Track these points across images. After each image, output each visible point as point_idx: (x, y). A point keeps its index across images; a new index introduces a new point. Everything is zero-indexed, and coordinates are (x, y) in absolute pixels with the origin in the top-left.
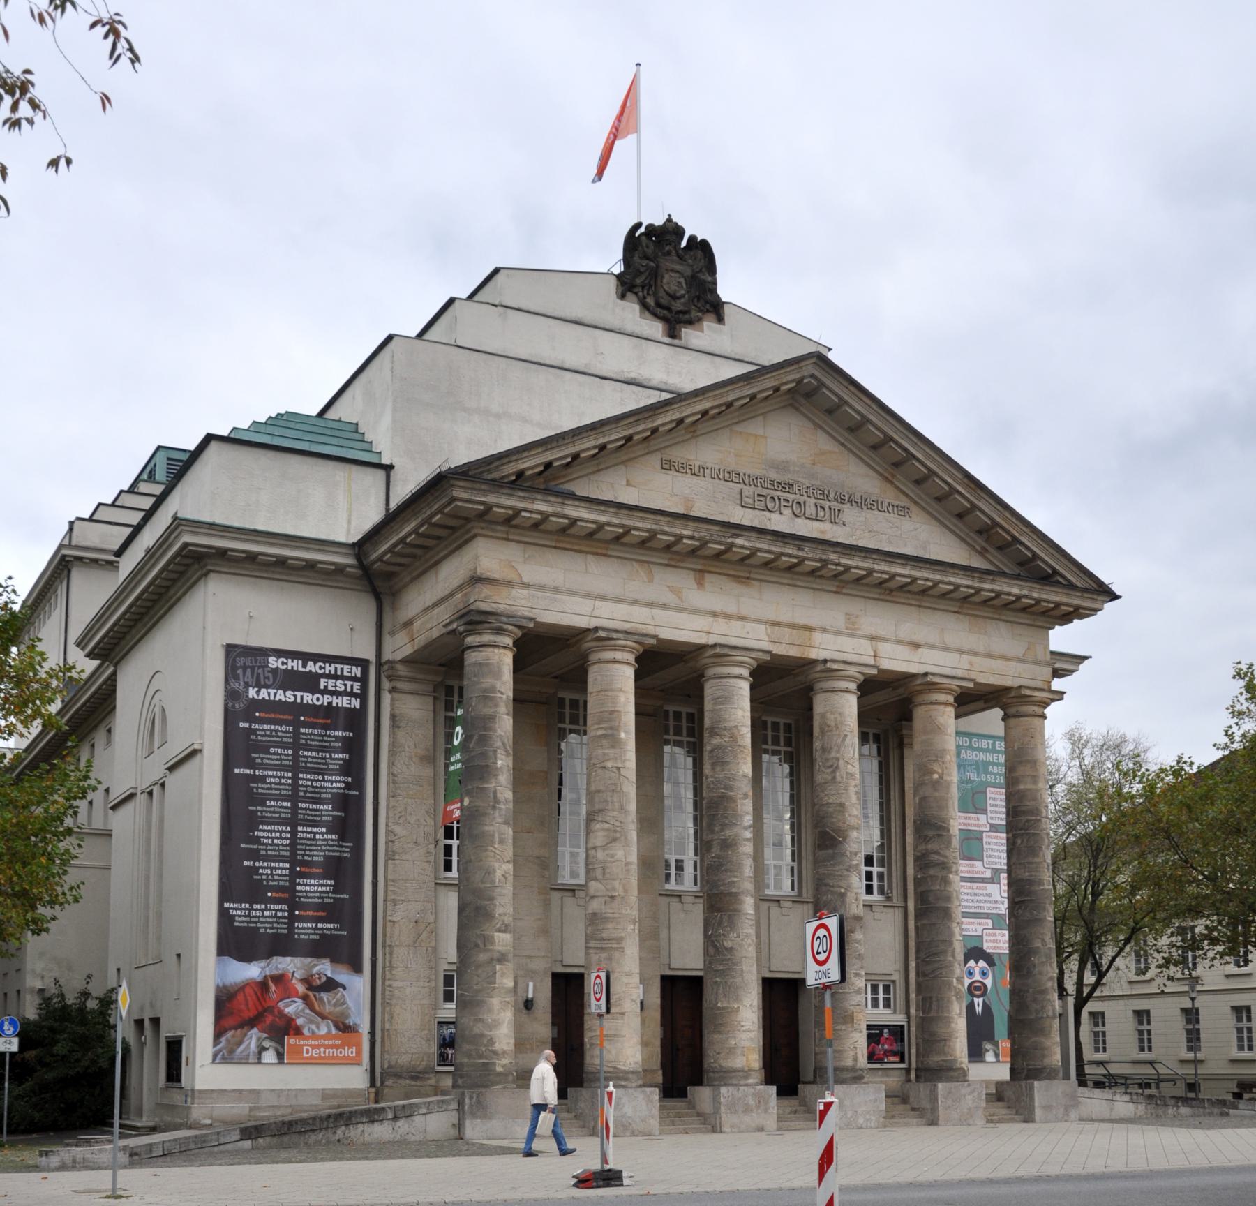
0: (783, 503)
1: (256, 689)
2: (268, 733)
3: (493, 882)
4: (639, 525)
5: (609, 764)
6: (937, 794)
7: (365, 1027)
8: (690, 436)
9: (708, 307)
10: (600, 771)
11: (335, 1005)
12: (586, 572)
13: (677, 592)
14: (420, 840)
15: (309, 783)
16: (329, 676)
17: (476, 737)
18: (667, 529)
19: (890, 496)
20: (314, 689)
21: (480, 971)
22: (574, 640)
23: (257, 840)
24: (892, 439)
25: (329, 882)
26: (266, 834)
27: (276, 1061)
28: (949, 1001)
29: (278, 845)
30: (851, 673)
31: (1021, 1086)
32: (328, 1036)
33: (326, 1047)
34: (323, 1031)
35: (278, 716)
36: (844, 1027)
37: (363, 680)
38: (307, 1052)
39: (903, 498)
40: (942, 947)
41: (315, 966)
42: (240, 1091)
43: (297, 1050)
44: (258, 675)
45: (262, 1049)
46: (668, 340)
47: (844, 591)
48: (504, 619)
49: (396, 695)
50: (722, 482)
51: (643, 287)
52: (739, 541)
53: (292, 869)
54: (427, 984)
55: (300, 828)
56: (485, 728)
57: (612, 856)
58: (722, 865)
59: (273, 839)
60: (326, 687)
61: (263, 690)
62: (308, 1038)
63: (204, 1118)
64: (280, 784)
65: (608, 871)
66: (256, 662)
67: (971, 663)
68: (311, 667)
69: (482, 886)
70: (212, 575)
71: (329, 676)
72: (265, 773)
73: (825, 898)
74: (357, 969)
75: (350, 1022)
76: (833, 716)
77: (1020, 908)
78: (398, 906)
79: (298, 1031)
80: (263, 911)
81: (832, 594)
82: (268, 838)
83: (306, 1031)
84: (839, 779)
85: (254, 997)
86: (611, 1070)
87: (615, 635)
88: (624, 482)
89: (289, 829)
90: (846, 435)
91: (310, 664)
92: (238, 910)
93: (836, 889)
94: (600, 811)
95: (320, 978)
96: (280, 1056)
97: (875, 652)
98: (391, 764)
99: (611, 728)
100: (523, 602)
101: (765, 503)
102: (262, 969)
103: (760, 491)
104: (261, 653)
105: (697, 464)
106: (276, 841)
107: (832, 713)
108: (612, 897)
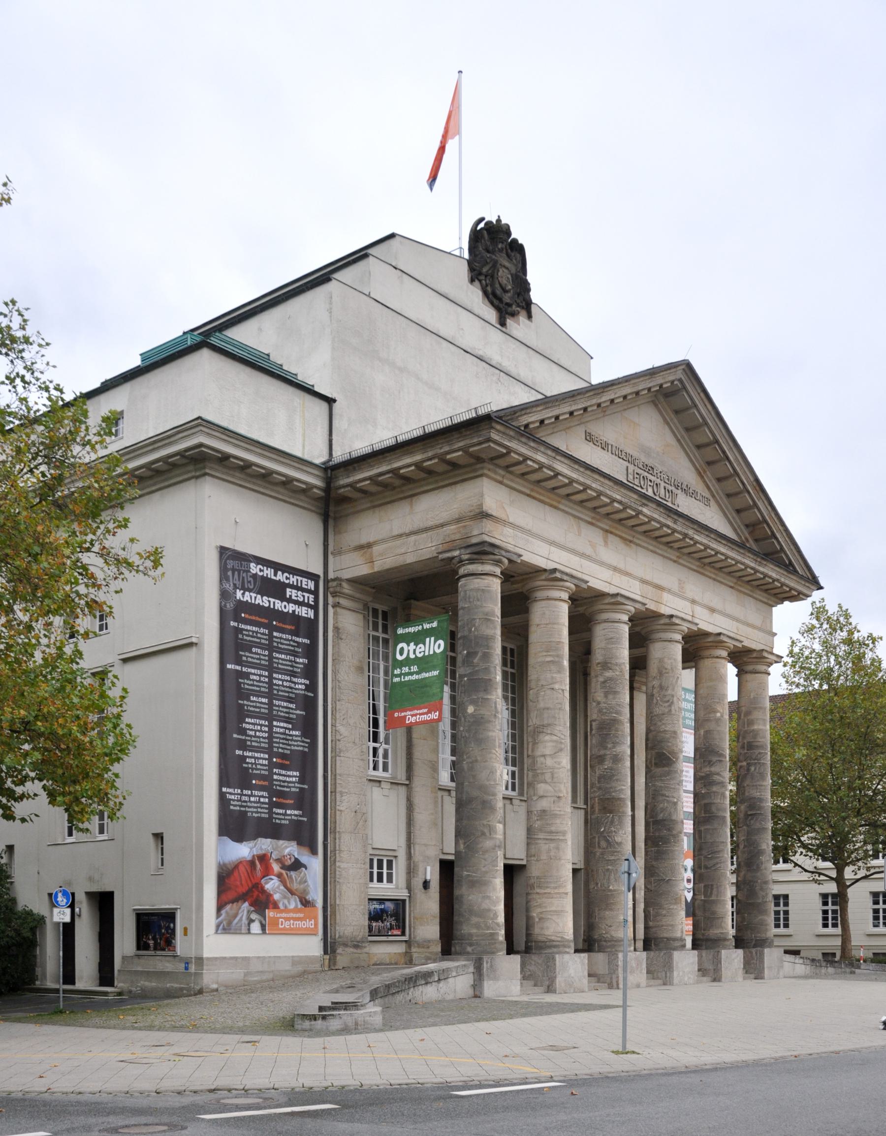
0: (649, 483)
1: (242, 591)
2: (251, 633)
3: (495, 780)
4: (594, 485)
5: (557, 686)
6: (719, 728)
7: (319, 903)
9: (524, 304)
10: (549, 692)
11: (300, 883)
12: (545, 520)
13: (593, 545)
14: (357, 741)
15: (280, 683)
16: (292, 587)
17: (480, 654)
18: (608, 492)
19: (700, 488)
20: (283, 598)
21: (486, 856)
22: (521, 578)
23: (243, 732)
24: (717, 442)
25: (295, 773)
26: (251, 727)
27: (260, 932)
28: (725, 888)
29: (259, 737)
31: (751, 952)
32: (295, 910)
33: (295, 919)
34: (292, 906)
35: (257, 619)
36: (675, 907)
37: (315, 593)
38: (282, 924)
39: (706, 491)
40: (721, 847)
41: (286, 847)
42: (236, 958)
43: (275, 922)
44: (243, 578)
45: (251, 921)
46: (499, 326)
47: (681, 561)
48: (503, 553)
49: (338, 609)
50: (617, 458)
51: (486, 276)
52: (645, 510)
53: (270, 760)
54: (363, 866)
55: (275, 723)
56: (488, 647)
57: (559, 763)
58: (613, 775)
59: (256, 731)
60: (291, 596)
61: (247, 593)
62: (282, 911)
63: (213, 983)
64: (259, 681)
65: (556, 775)
66: (241, 564)
68: (281, 577)
69: (487, 783)
70: (207, 478)
71: (292, 587)
72: (249, 670)
73: (661, 805)
74: (314, 852)
75: (309, 897)
76: (669, 662)
77: (752, 819)
78: (343, 798)
79: (276, 906)
80: (249, 796)
81: (671, 563)
82: (252, 730)
84: (673, 712)
85: (246, 874)
86: (559, 939)
87: (565, 578)
89: (267, 723)
90: (683, 432)
92: (233, 794)
93: (671, 799)
94: (549, 725)
95: (290, 859)
96: (263, 927)
98: (335, 672)
99: (558, 656)
100: (510, 540)
102: (251, 849)
104: (244, 558)
106: (258, 734)
107: (669, 659)
108: (559, 797)
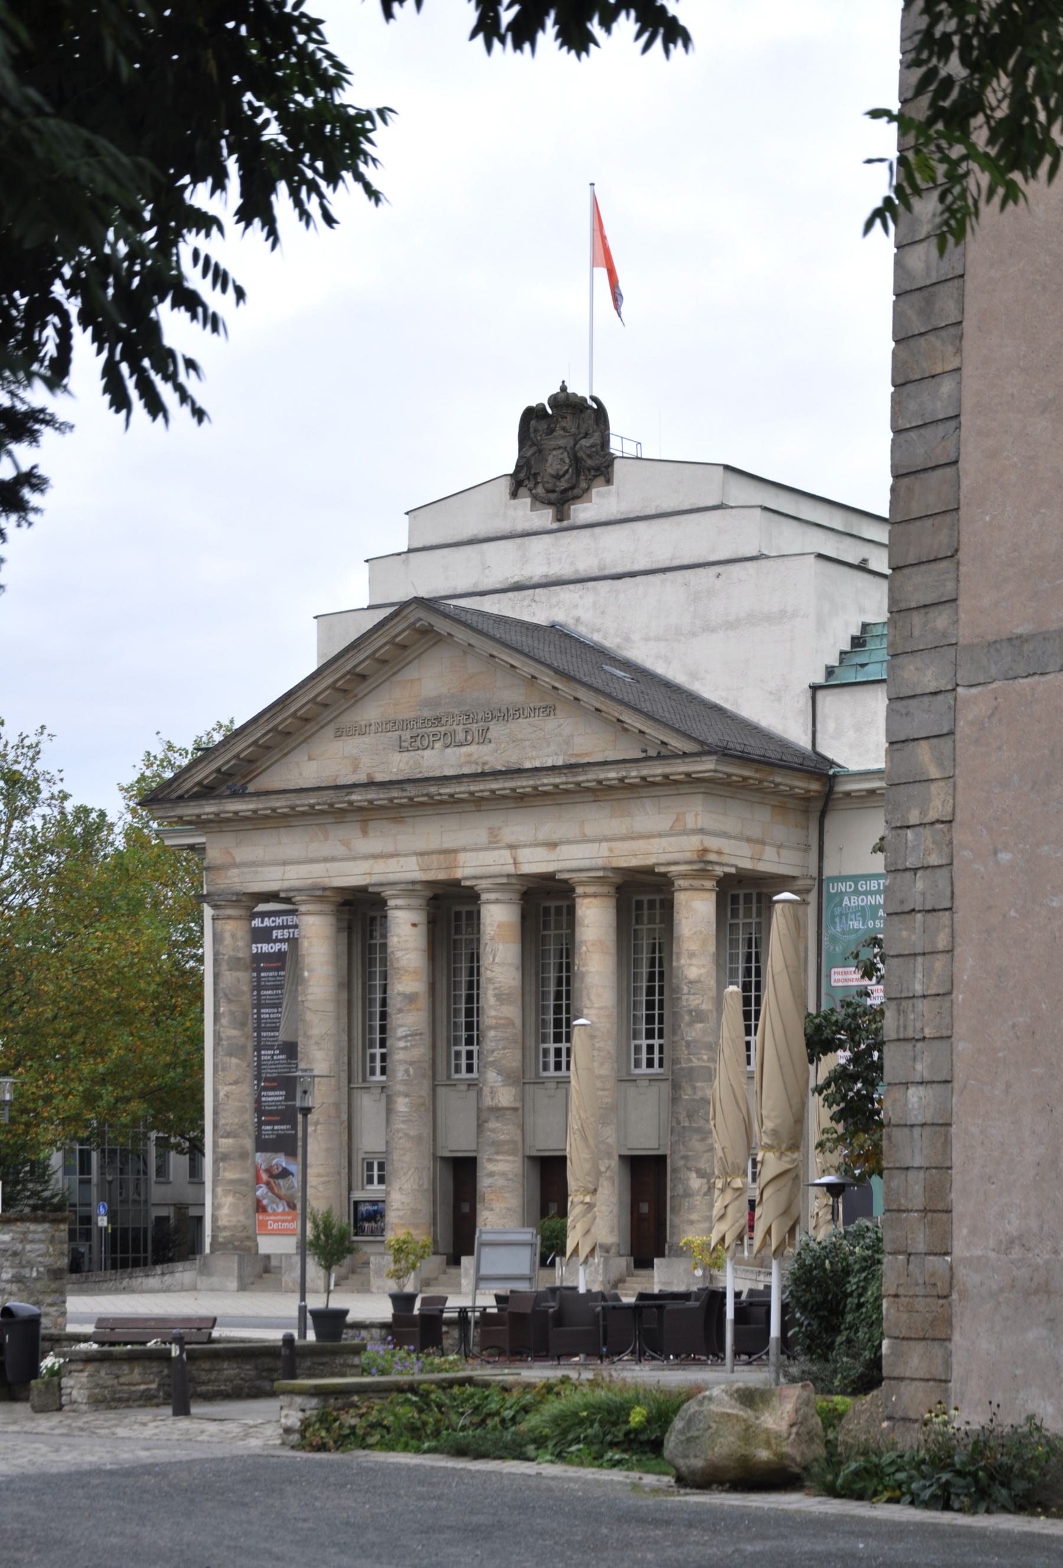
8: (352, 701)
11: (288, 1189)
12: (280, 843)
13: (346, 843)
30: (484, 886)
32: (283, 1213)
33: (283, 1221)
34: (280, 1210)
48: (216, 898)
52: (354, 797)
62: (270, 1215)
67: (611, 850)
83: (269, 1210)
88: (306, 758)
91: (266, 919)
97: (515, 859)
100: (236, 880)
101: (417, 743)
103: (414, 733)
105: (363, 723)
